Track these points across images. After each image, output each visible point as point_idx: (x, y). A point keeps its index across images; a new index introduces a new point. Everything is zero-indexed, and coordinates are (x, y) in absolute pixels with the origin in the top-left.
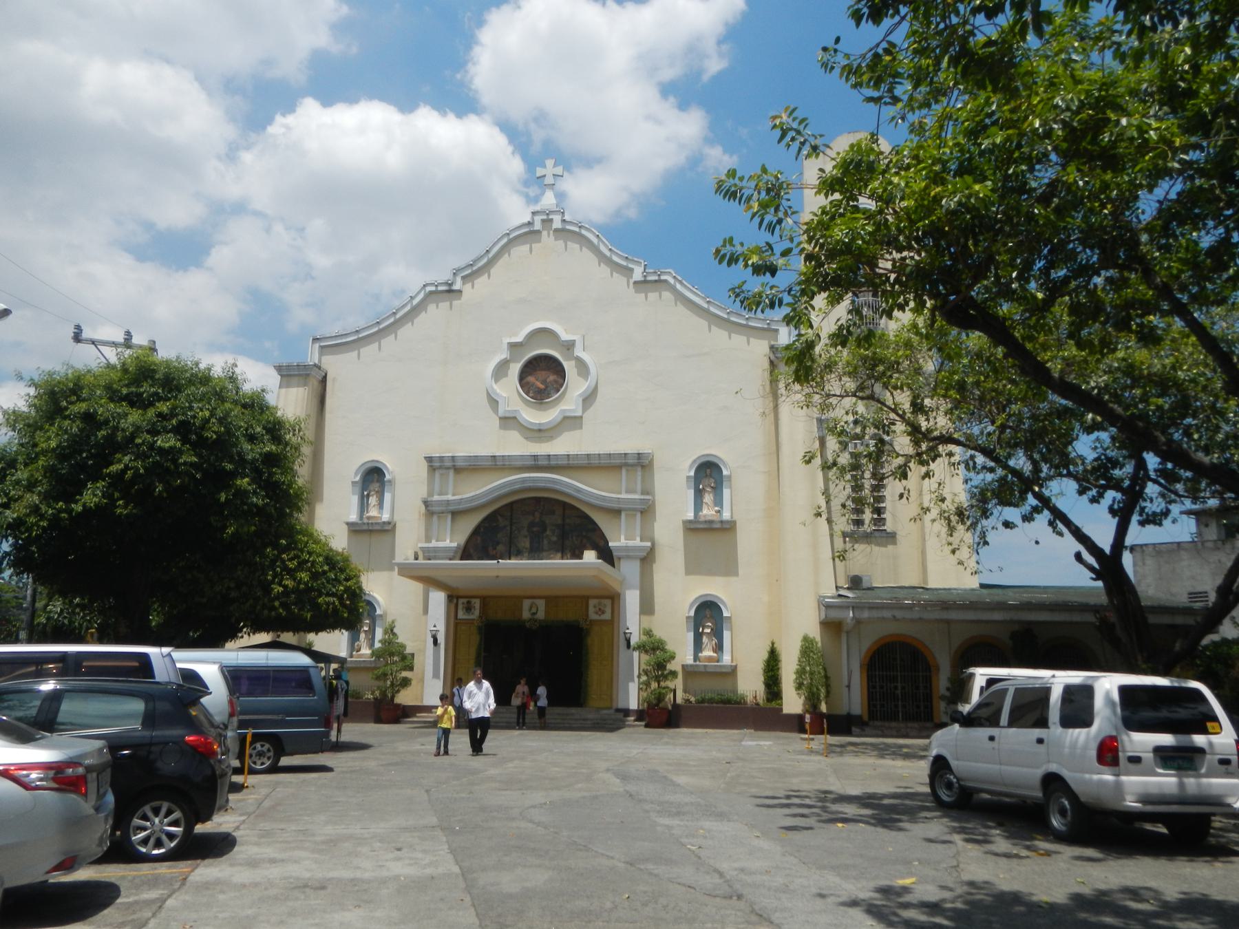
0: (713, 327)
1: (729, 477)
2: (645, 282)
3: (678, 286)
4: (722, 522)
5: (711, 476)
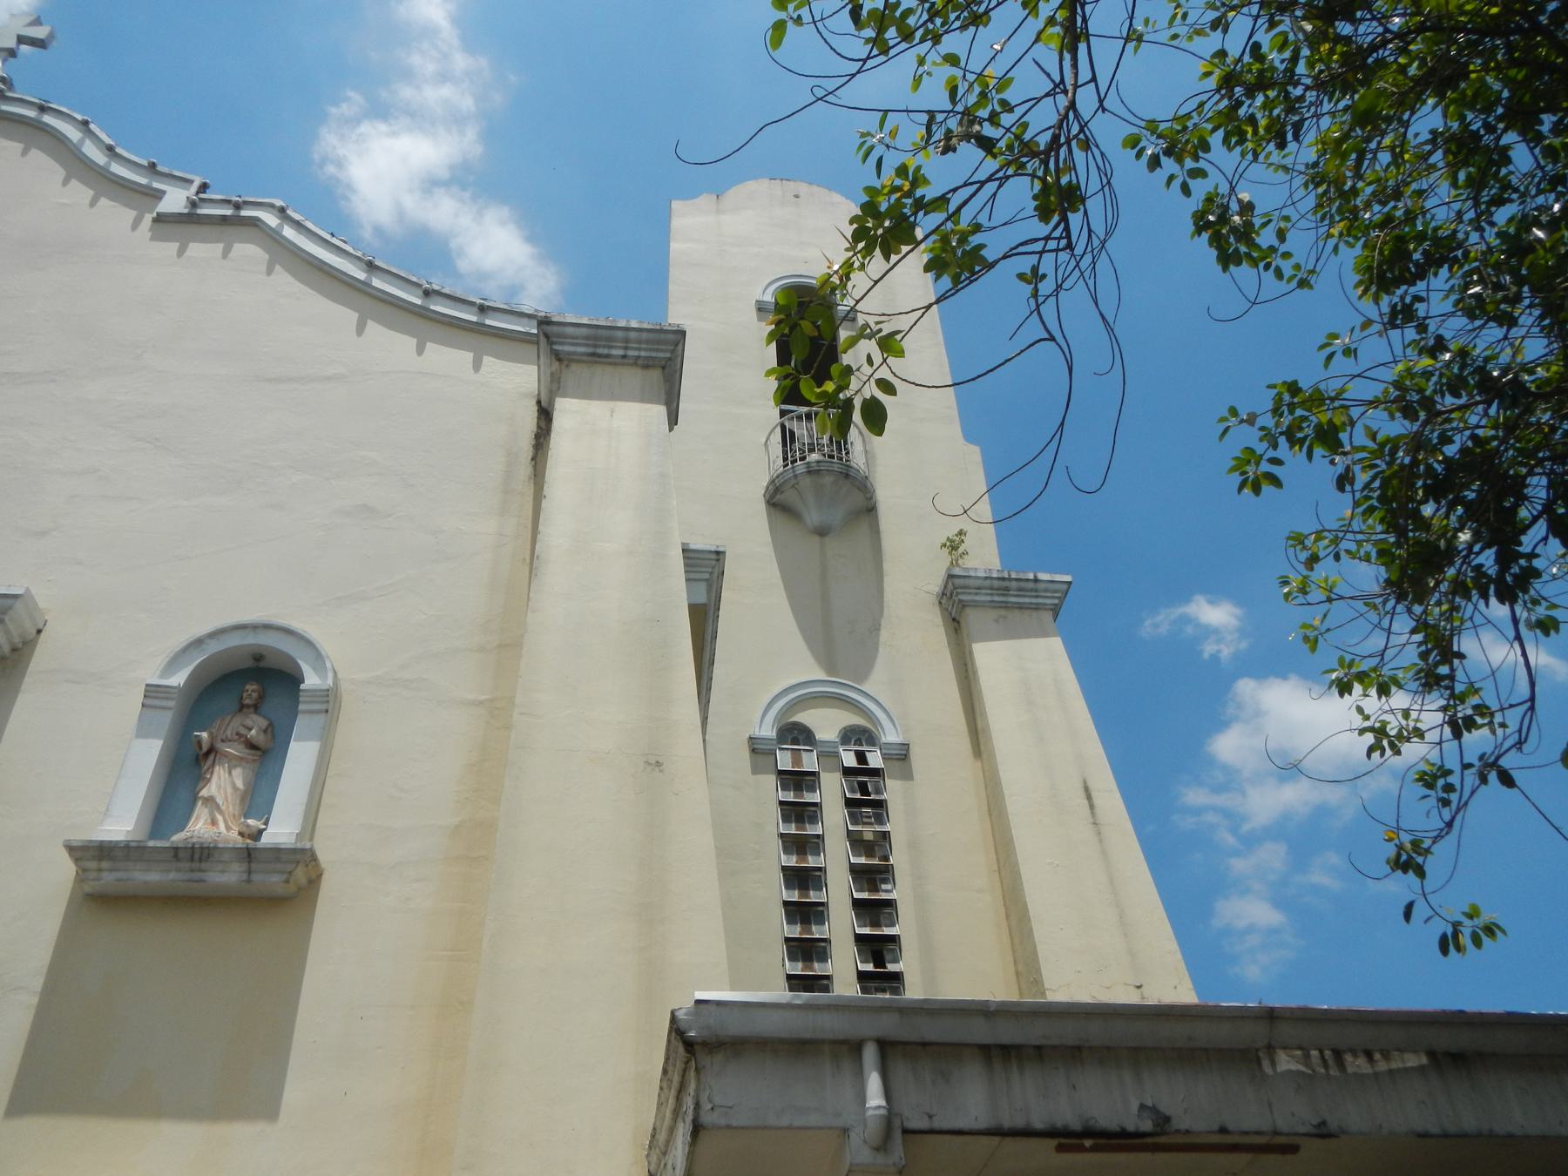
0: (372, 326)
1: (328, 701)
2: (190, 219)
3: (289, 232)
4: (251, 855)
5: (256, 708)
